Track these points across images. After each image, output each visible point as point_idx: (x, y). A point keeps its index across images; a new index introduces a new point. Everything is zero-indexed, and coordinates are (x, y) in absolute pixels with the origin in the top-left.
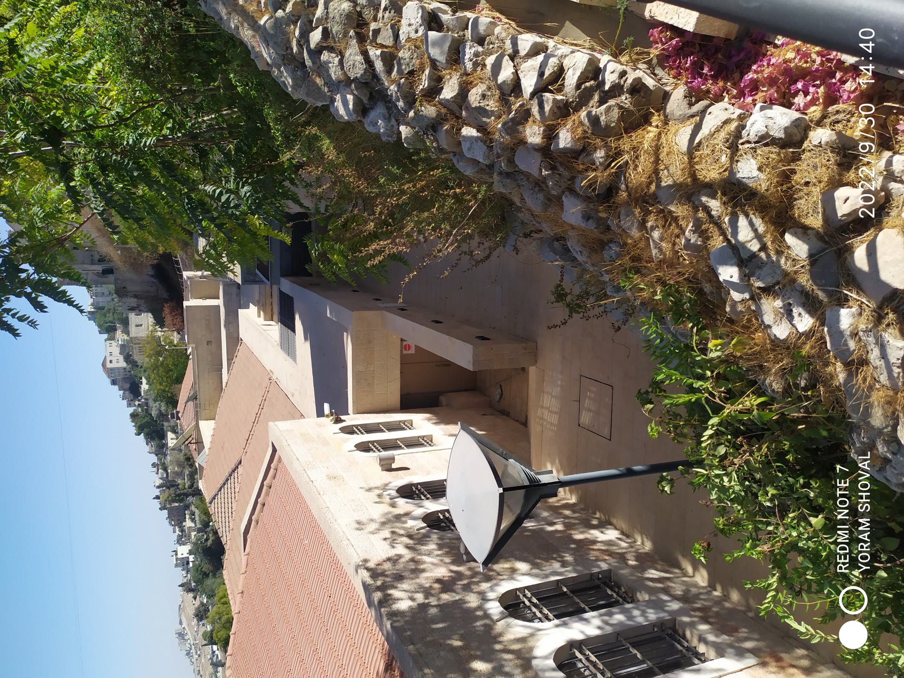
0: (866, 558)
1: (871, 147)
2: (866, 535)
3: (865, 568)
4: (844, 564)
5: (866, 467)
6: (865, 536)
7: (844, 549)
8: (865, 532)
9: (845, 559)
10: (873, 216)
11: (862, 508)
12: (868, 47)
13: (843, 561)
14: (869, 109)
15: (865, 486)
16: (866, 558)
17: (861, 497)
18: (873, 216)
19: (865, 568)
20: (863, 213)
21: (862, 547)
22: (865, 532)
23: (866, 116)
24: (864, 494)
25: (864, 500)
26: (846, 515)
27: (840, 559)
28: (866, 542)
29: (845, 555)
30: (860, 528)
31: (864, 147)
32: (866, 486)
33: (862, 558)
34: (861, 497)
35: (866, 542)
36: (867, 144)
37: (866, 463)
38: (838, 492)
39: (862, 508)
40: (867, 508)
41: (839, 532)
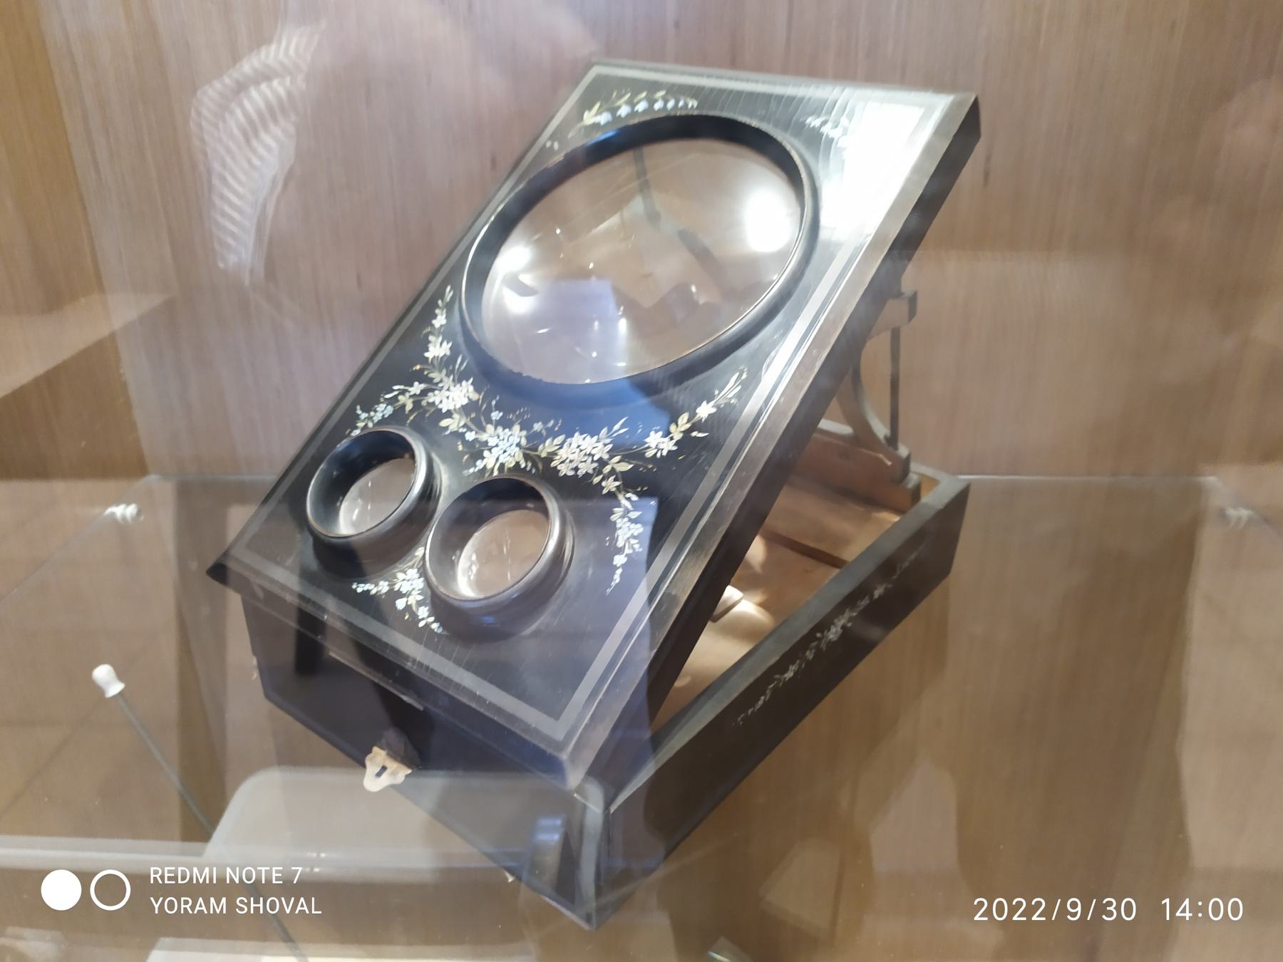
0: (171, 908)
1: (1074, 915)
2: (204, 908)
3: (157, 906)
4: (162, 877)
5: (299, 908)
6: (200, 906)
7: (183, 879)
8: (208, 909)
9: (170, 879)
10: (977, 918)
11: (242, 902)
12: (1184, 911)
13: (166, 875)
14: (1128, 913)
15: (273, 906)
16: (171, 908)
17: (257, 902)
18: (977, 918)
19: (157, 906)
20: (981, 904)
21: (186, 902)
22: (208, 909)
23: (1118, 908)
24: (261, 905)
25: (252, 905)
26: (232, 879)
27: (169, 872)
28: (193, 908)
29: (175, 878)
30: (212, 900)
31: (1074, 905)
32: (273, 908)
33: (171, 903)
34: (257, 902)
35: (193, 908)
36: (1079, 909)
37: (305, 908)
38: (263, 869)
39: (242, 902)
40: (242, 909)
41: (207, 870)
